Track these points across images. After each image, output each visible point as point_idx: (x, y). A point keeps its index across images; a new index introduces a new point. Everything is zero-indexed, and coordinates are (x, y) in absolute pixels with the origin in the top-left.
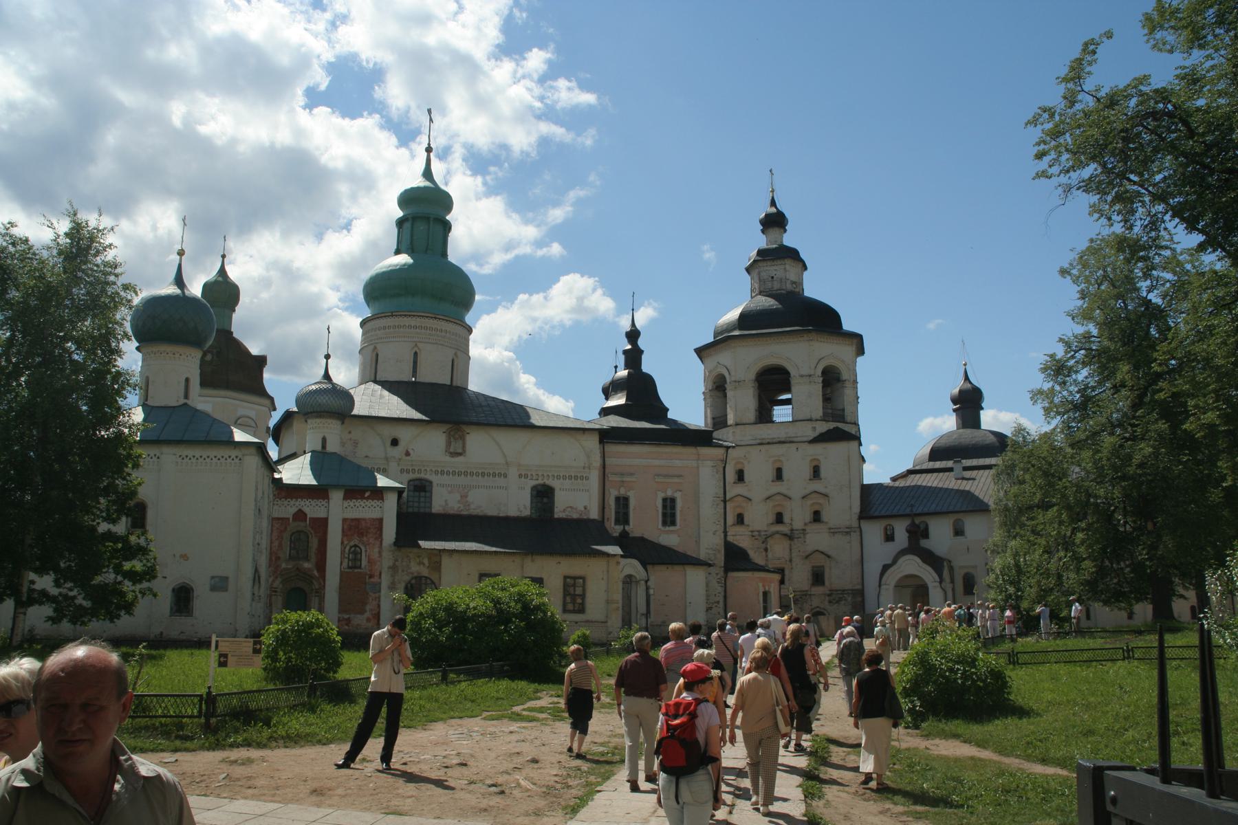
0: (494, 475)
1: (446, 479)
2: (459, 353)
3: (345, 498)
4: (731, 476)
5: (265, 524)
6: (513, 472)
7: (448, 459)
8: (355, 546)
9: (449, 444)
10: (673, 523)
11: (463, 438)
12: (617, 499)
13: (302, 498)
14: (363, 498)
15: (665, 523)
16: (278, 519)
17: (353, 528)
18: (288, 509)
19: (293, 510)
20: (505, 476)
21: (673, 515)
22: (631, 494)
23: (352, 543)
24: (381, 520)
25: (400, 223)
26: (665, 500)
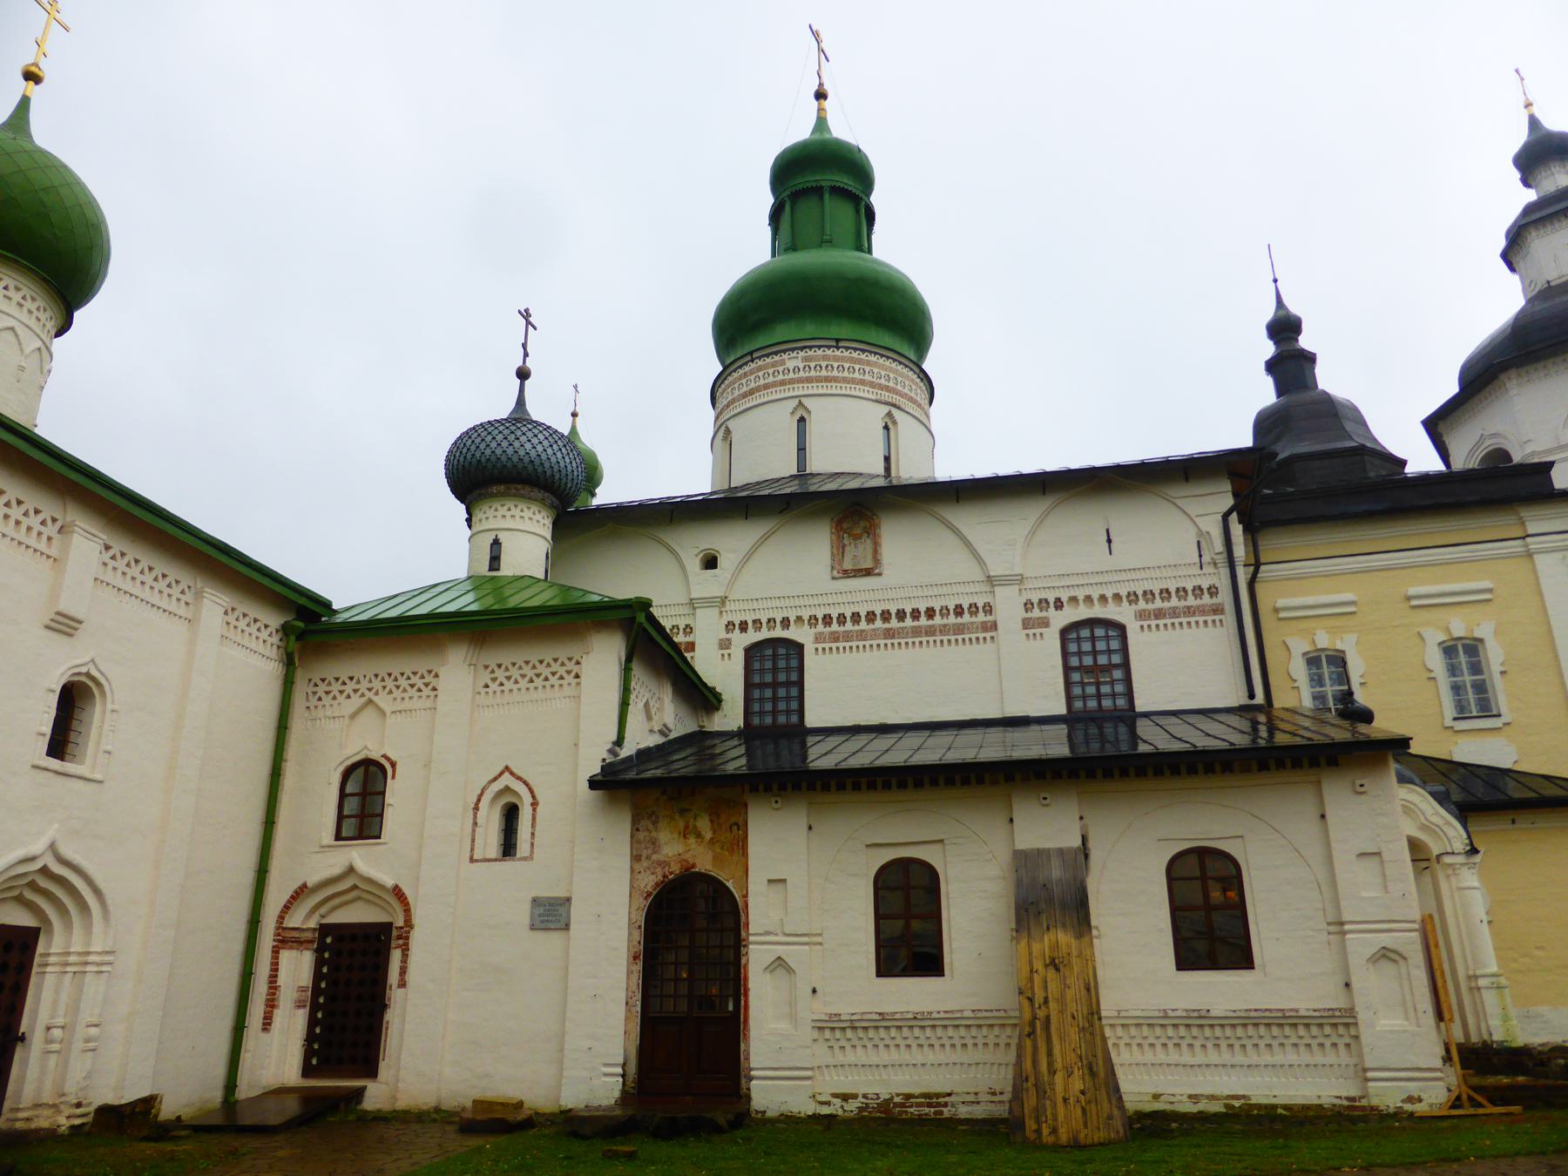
9: (839, 551)
25: (775, 217)
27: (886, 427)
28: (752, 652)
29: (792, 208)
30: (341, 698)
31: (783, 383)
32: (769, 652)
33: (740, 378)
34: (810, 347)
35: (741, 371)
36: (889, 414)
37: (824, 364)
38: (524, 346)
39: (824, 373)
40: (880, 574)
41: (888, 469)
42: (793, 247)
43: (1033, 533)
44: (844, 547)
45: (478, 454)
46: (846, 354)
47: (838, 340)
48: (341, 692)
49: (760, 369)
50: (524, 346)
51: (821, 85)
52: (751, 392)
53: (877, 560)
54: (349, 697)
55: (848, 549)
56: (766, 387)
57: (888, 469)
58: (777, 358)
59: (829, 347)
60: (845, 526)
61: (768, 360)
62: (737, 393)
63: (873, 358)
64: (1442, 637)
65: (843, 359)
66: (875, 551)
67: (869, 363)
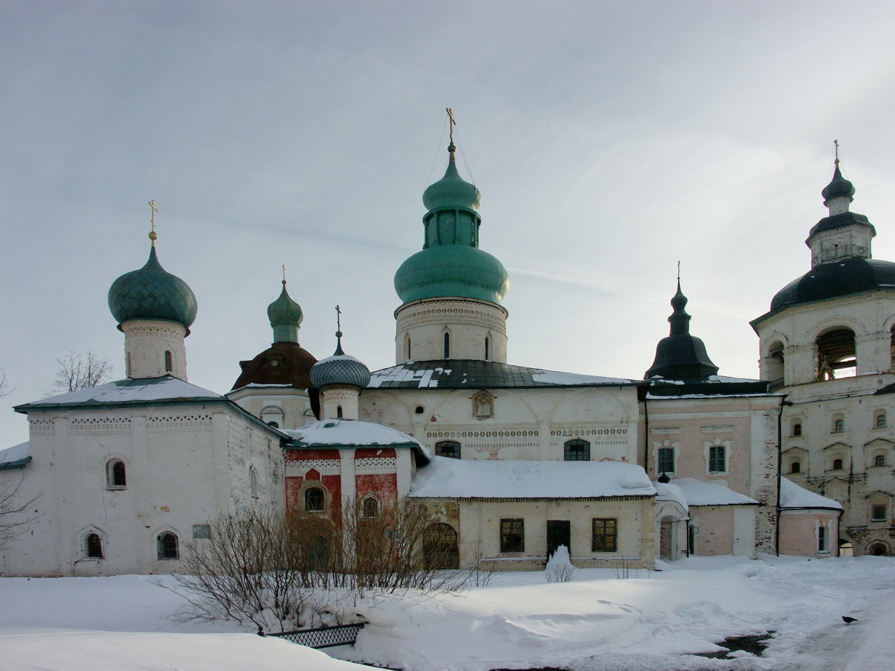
0: (525, 434)
2: (492, 332)
4: (787, 429)
5: (281, 486)
6: (545, 431)
7: (476, 421)
9: (476, 408)
10: (722, 469)
11: (490, 402)
12: (662, 451)
13: (313, 459)
15: (712, 469)
16: (292, 478)
17: (366, 482)
18: (301, 469)
19: (307, 470)
20: (537, 434)
21: (722, 463)
22: (676, 447)
23: (366, 497)
25: (427, 220)
26: (712, 449)
36: (489, 332)
51: (452, 143)
64: (711, 445)
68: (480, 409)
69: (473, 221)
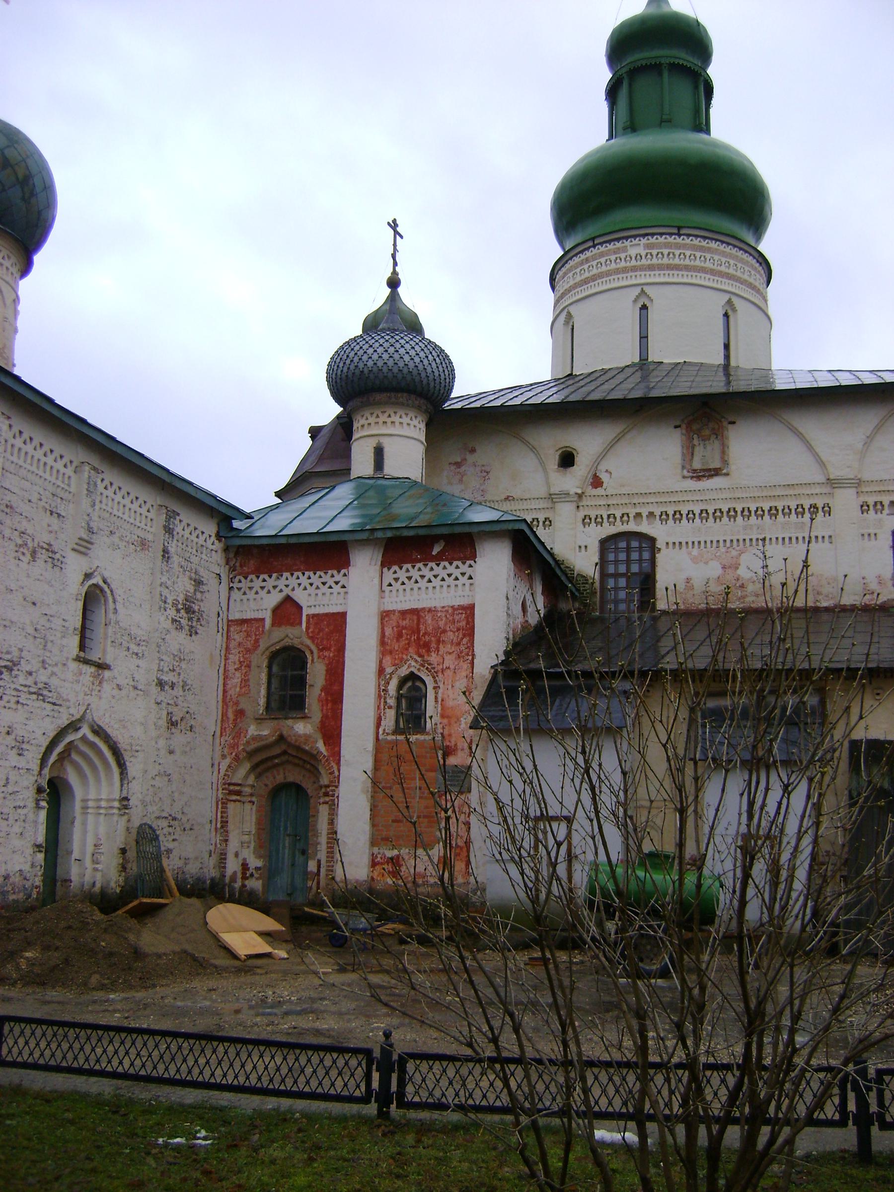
1: (684, 531)
3: (386, 563)
8: (412, 677)
9: (689, 452)
14: (427, 558)
18: (260, 599)
19: (275, 599)
20: (828, 510)
23: (404, 671)
24: (469, 610)
25: (612, 93)
27: (726, 315)
28: (606, 544)
29: (630, 85)
30: (263, 593)
31: (625, 270)
32: (623, 545)
33: (582, 263)
34: (653, 235)
35: (583, 256)
37: (666, 252)
38: (394, 256)
39: (665, 261)
40: (727, 474)
41: (727, 357)
42: (632, 127)
43: (870, 439)
44: (693, 446)
45: (361, 365)
46: (688, 241)
47: (679, 228)
48: (262, 588)
49: (602, 255)
50: (394, 256)
52: (594, 278)
53: (725, 462)
54: (269, 592)
55: (697, 449)
56: (608, 274)
57: (727, 357)
58: (619, 245)
59: (671, 234)
60: (695, 427)
61: (611, 247)
62: (578, 278)
63: (713, 245)
65: (684, 246)
66: (723, 453)
67: (709, 250)
68: (699, 451)
69: (696, 87)
